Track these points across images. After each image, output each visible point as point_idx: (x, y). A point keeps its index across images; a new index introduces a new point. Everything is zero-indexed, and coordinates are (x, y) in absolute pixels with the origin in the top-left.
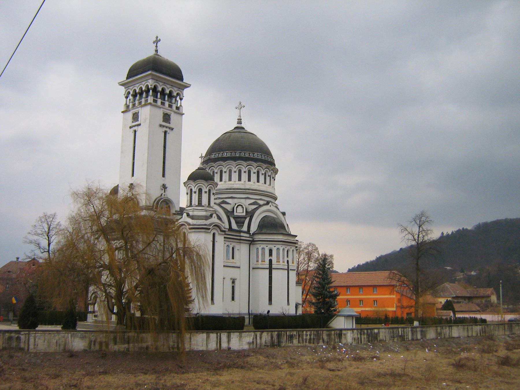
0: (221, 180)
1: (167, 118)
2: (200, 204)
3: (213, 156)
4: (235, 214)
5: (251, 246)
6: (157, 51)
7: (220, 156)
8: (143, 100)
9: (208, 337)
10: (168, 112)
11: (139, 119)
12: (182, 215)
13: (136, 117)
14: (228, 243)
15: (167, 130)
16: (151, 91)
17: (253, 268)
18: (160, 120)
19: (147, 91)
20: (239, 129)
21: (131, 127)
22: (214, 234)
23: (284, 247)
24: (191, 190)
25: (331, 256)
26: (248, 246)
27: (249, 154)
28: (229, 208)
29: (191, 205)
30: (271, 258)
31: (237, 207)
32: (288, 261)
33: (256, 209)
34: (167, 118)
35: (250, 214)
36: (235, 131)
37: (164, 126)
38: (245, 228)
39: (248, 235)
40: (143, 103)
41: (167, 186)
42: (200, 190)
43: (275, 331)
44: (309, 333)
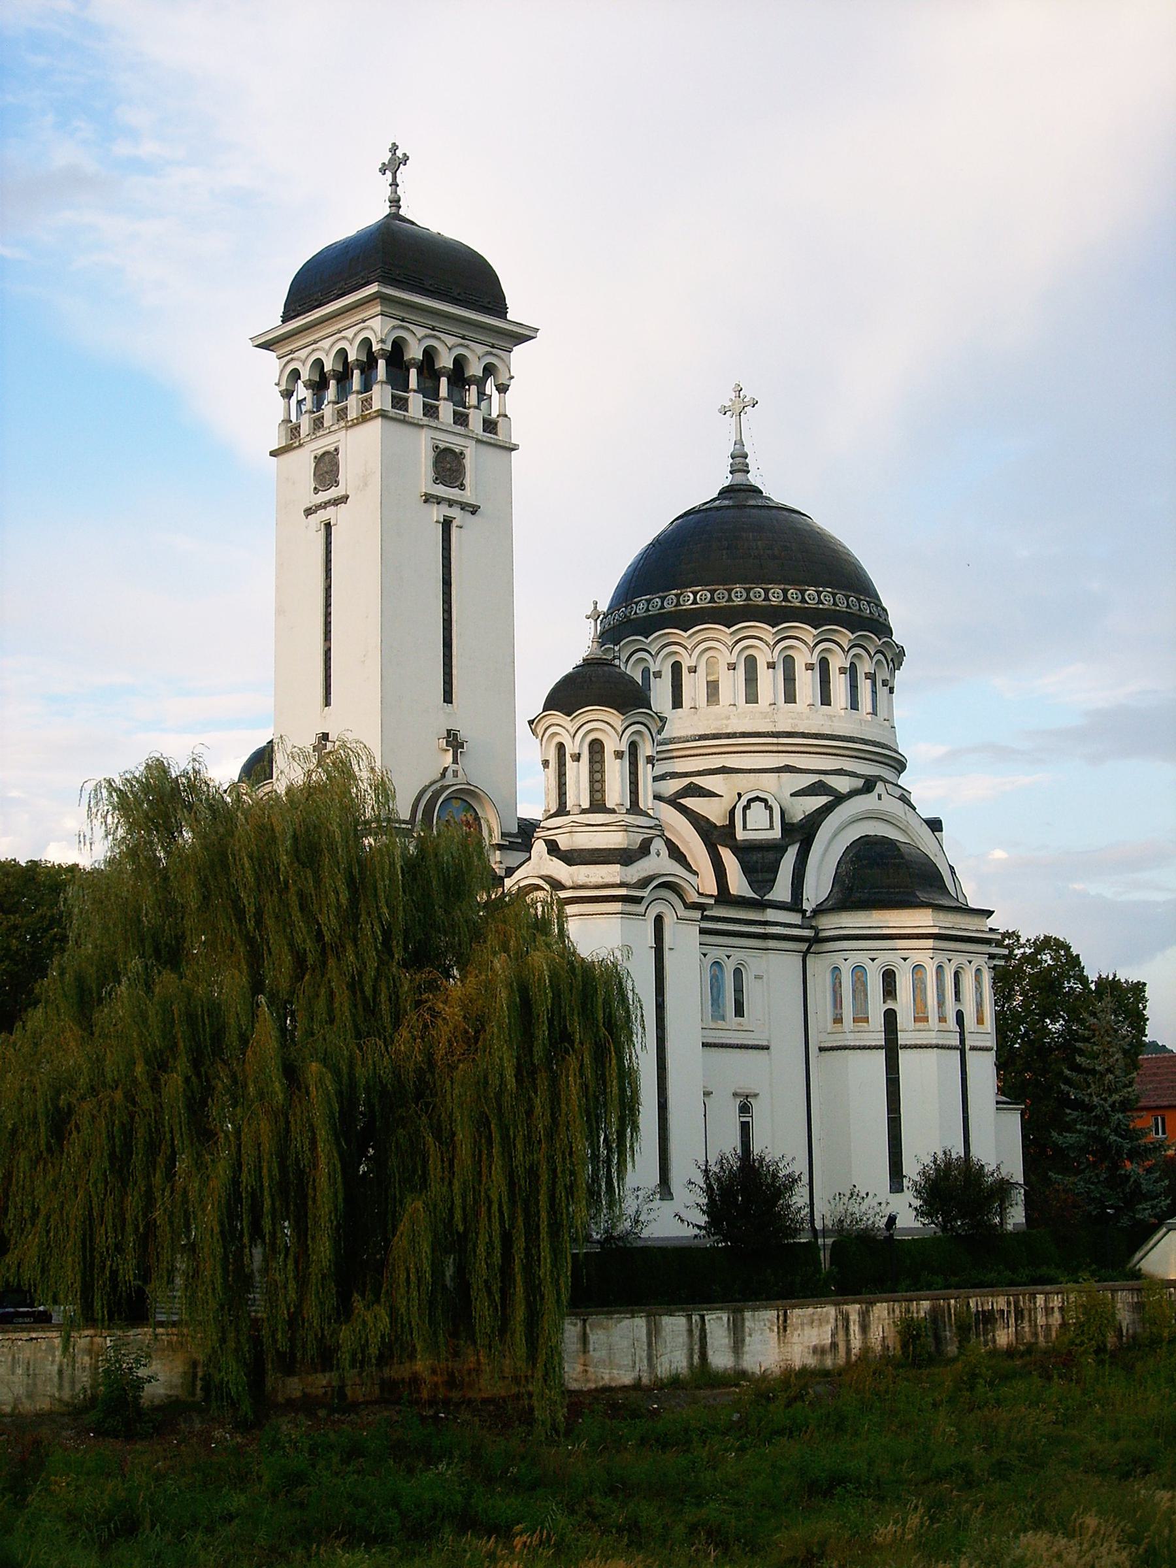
0: (677, 703)
1: (448, 466)
2: (597, 805)
3: (639, 609)
4: (740, 835)
5: (810, 959)
6: (395, 202)
7: (669, 607)
8: (353, 403)
9: (654, 1332)
10: (454, 442)
11: (341, 478)
12: (528, 847)
13: (327, 469)
14: (716, 954)
15: (454, 512)
16: (381, 363)
17: (821, 1049)
18: (423, 477)
19: (368, 366)
20: (740, 494)
21: (309, 512)
22: (659, 920)
23: (942, 957)
24: (561, 747)
25: (1139, 988)
26: (797, 960)
27: (785, 592)
28: (713, 811)
29: (562, 811)
30: (890, 1005)
31: (746, 808)
32: (960, 1016)
33: (827, 810)
34: (448, 466)
35: (802, 833)
36: (726, 502)
37: (439, 500)
38: (781, 891)
39: (795, 918)
40: (352, 414)
41: (462, 736)
42: (596, 748)
43: (919, 1299)
44: (1056, 1301)
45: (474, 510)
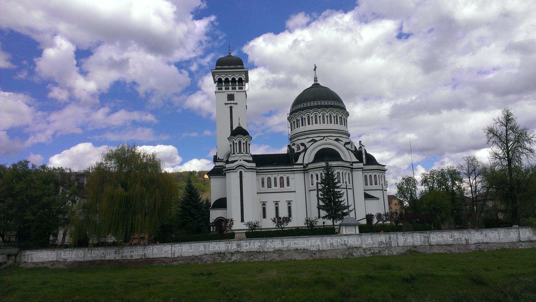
1: (231, 97)
14: (260, 177)
20: (316, 85)
34: (231, 97)
37: (228, 104)
38: (300, 161)
39: (302, 166)
45: (236, 104)
